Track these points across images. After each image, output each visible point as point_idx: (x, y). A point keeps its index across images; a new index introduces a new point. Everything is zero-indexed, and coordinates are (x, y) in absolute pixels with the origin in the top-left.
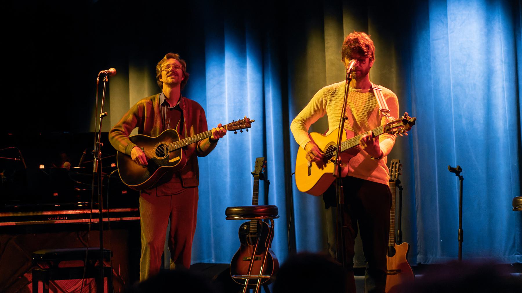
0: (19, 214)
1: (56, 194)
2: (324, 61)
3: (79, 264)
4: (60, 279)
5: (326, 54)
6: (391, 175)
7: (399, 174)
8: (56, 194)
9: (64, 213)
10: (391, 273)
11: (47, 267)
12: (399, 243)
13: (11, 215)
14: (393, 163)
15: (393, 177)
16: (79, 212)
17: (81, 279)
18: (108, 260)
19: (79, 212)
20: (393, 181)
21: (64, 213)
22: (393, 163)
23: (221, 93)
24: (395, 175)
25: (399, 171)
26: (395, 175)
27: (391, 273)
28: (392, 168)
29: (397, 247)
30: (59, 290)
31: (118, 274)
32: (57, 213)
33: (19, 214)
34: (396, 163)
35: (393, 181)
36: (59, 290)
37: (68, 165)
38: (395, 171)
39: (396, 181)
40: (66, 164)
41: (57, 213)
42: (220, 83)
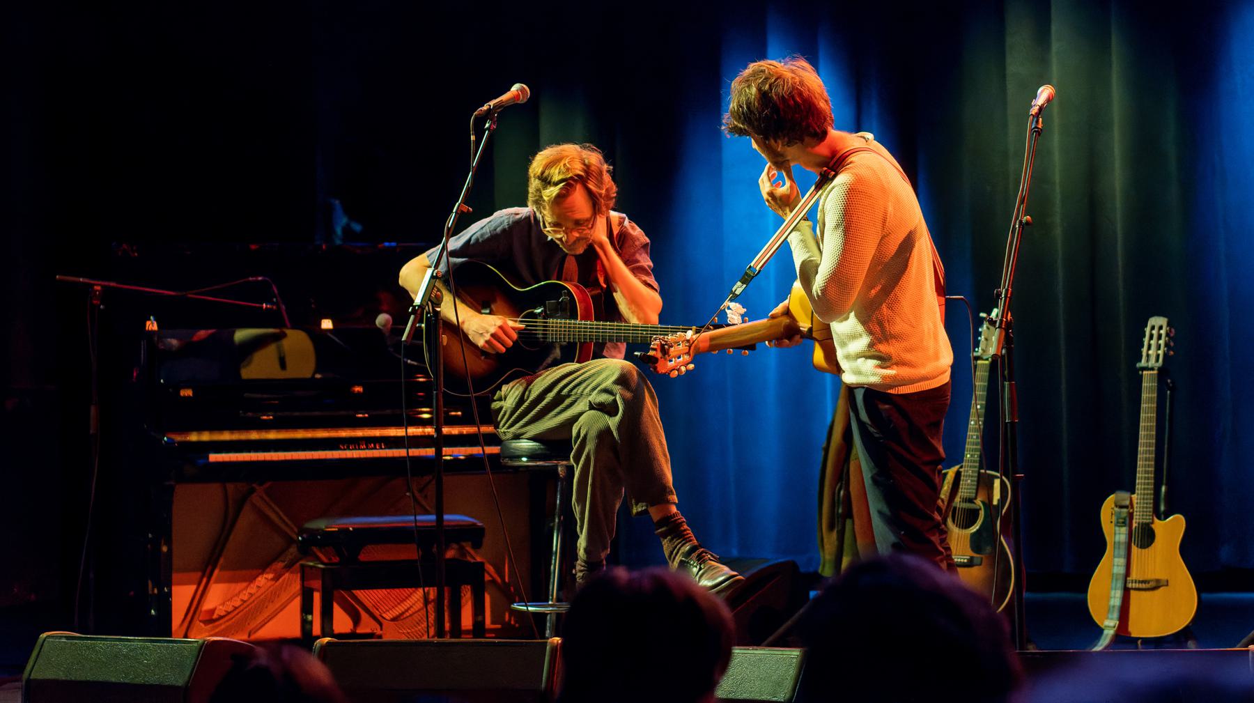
0: (272, 435)
1: (358, 389)
2: (1003, 77)
3: (409, 553)
4: (363, 589)
5: (1009, 60)
6: (1148, 355)
7: (1165, 355)
8: (358, 389)
9: (377, 432)
10: (1144, 586)
11: (336, 560)
13: (254, 436)
14: (1153, 328)
16: (413, 431)
17: (416, 585)
18: (477, 545)
19: (413, 431)
20: (1152, 369)
21: (377, 432)
22: (1153, 328)
24: (1158, 356)
25: (1167, 345)
26: (1158, 356)
27: (1144, 586)
28: (1151, 337)
29: (1158, 526)
30: (364, 615)
31: (503, 578)
32: (359, 433)
33: (272, 435)
34: (1161, 328)
35: (1152, 369)
36: (364, 615)
37: (387, 321)
38: (1159, 347)
39: (1160, 369)
40: (382, 319)
41: (359, 433)
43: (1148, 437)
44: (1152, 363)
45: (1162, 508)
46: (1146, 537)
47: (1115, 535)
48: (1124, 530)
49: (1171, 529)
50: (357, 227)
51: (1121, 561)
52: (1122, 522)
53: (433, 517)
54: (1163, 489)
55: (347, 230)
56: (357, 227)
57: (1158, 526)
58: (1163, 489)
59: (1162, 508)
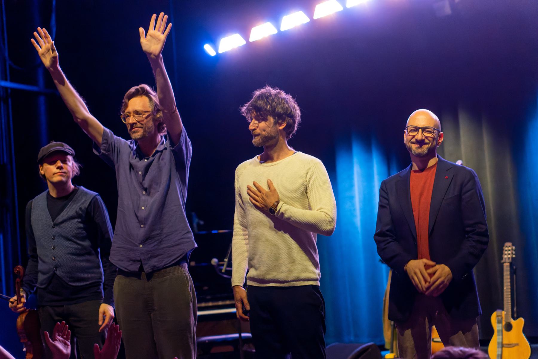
12: (517, 318)
15: (507, 261)
23: (352, 186)
25: (512, 253)
29: (513, 322)
40: (214, 261)
42: (350, 177)
43: (507, 289)
44: (507, 261)
45: (515, 315)
46: (509, 327)
47: (496, 326)
48: (500, 325)
49: (519, 324)
50: (202, 223)
51: (500, 337)
52: (499, 322)
53: (237, 335)
54: (515, 309)
55: (198, 224)
56: (202, 223)
57: (513, 322)
58: (515, 309)
59: (515, 315)
